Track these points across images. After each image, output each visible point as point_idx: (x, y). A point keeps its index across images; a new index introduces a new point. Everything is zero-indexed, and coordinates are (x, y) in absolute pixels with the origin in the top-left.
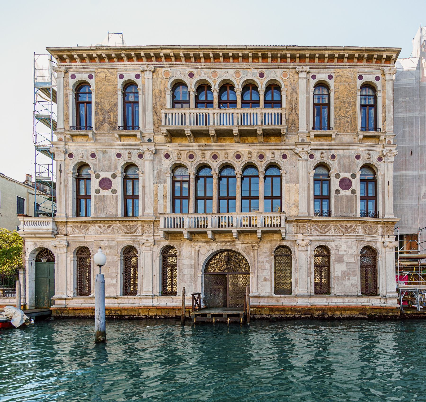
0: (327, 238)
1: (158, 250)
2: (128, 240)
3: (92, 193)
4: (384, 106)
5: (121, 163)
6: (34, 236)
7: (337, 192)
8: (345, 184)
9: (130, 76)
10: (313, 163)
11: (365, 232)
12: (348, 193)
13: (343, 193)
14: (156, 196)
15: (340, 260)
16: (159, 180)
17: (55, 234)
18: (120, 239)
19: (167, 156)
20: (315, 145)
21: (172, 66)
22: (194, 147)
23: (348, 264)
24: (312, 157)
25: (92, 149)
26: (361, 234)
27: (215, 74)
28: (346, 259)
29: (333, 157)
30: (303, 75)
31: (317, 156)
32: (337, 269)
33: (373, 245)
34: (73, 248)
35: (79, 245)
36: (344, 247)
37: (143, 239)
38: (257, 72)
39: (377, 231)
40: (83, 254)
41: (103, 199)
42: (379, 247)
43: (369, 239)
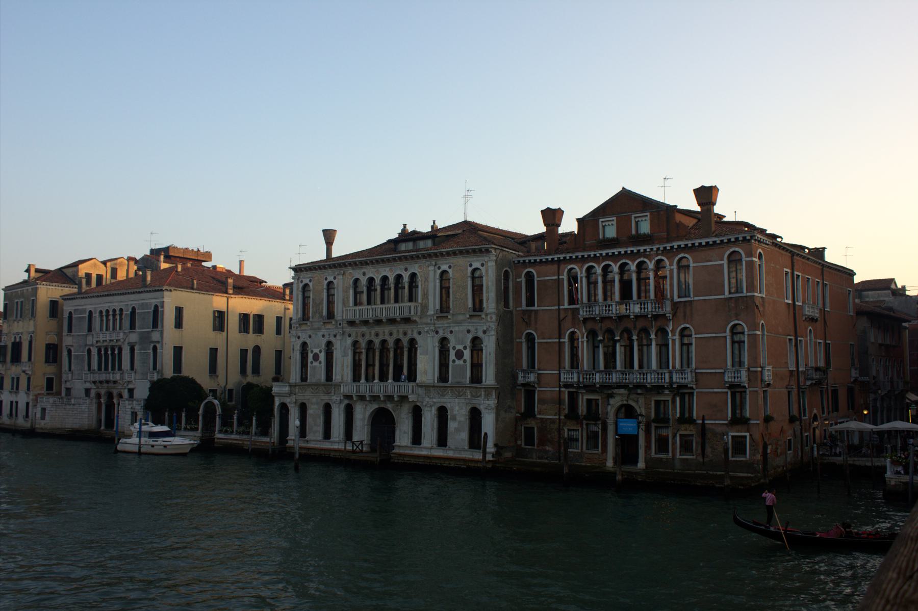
0: (445, 400)
1: (343, 406)
2: (326, 398)
3: (309, 364)
4: (488, 288)
5: (324, 341)
6: (280, 395)
7: (454, 361)
8: (459, 355)
9: (330, 278)
10: (437, 338)
11: (472, 396)
12: (461, 362)
13: (458, 362)
14: (343, 366)
15: (454, 418)
16: (345, 355)
17: (290, 394)
18: (323, 398)
19: (350, 336)
20: (439, 324)
21: (353, 269)
22: (364, 329)
23: (460, 422)
24: (437, 333)
25: (309, 333)
26: (469, 397)
27: (378, 272)
28: (458, 418)
29: (451, 332)
30: (431, 268)
31: (441, 332)
32: (452, 426)
33: (477, 406)
34: (298, 404)
35: (300, 401)
36: (457, 408)
37: (334, 398)
38: (403, 267)
39: (480, 395)
40: (303, 408)
41: (314, 368)
42: (482, 408)
43: (474, 402)
